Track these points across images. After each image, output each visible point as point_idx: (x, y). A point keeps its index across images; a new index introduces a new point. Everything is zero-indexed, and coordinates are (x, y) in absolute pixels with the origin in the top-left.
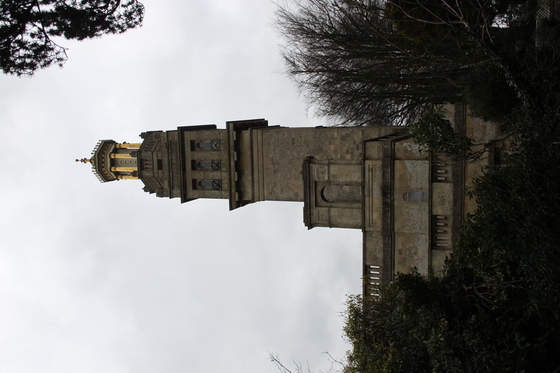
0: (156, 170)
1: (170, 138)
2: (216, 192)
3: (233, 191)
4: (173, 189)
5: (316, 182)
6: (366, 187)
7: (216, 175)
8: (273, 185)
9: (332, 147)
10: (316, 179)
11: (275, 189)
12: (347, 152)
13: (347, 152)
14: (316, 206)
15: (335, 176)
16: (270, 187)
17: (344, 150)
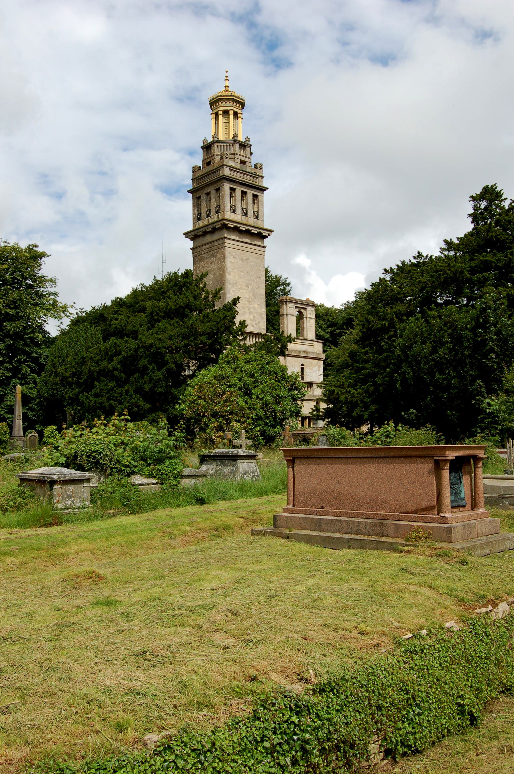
0: (240, 157)
1: (260, 178)
2: (229, 207)
3: (235, 224)
4: (230, 169)
5: (306, 309)
6: (306, 342)
7: (239, 210)
8: (235, 256)
9: (256, 306)
10: (307, 309)
11: (232, 257)
12: (254, 317)
13: (254, 317)
14: (296, 307)
15: (310, 321)
16: (233, 254)
17: (255, 315)
